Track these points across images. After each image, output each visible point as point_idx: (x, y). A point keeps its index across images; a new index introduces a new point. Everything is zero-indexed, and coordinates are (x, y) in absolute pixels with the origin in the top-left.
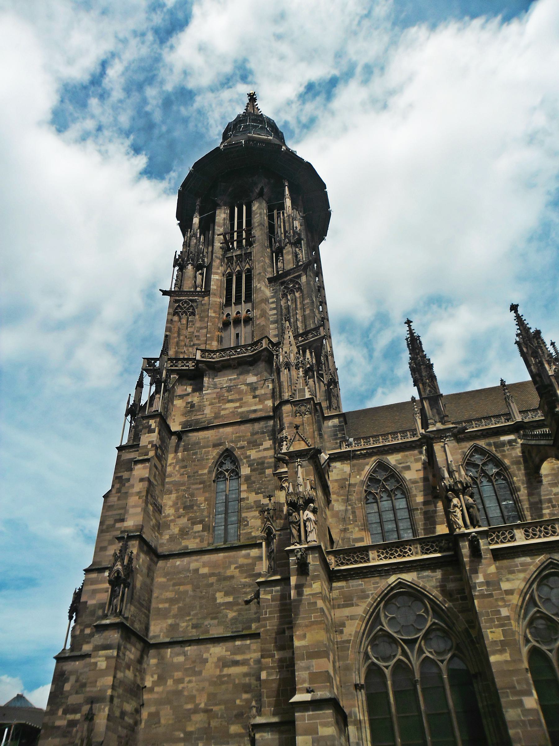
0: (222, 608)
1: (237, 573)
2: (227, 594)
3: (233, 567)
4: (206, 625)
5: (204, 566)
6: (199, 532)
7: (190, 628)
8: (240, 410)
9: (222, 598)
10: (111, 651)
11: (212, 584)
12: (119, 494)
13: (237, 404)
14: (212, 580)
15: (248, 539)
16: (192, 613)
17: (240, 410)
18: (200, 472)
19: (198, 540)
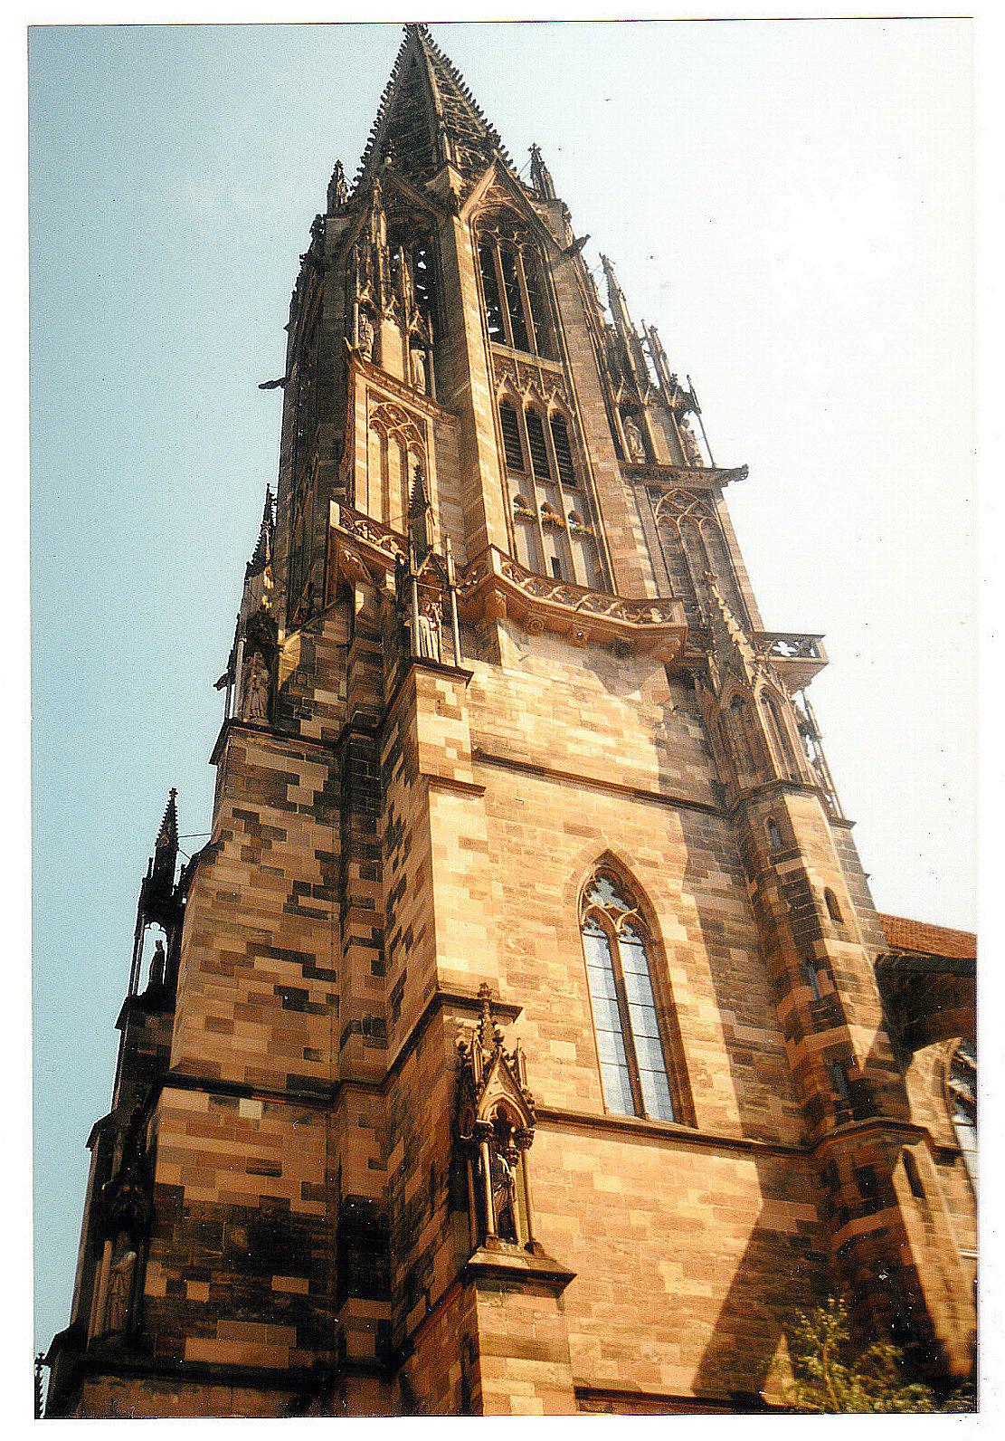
0: (686, 1311)
1: (706, 1213)
2: (690, 1272)
3: (694, 1195)
4: (647, 1356)
5: (605, 1167)
6: (568, 1063)
7: (596, 1353)
8: (619, 760)
9: (678, 1280)
10: (550, 1365)
11: (640, 1233)
12: (254, 867)
13: (610, 741)
14: (638, 1218)
15: (719, 1125)
16: (596, 1307)
17: (619, 760)
18: (540, 888)
19: (570, 1087)
